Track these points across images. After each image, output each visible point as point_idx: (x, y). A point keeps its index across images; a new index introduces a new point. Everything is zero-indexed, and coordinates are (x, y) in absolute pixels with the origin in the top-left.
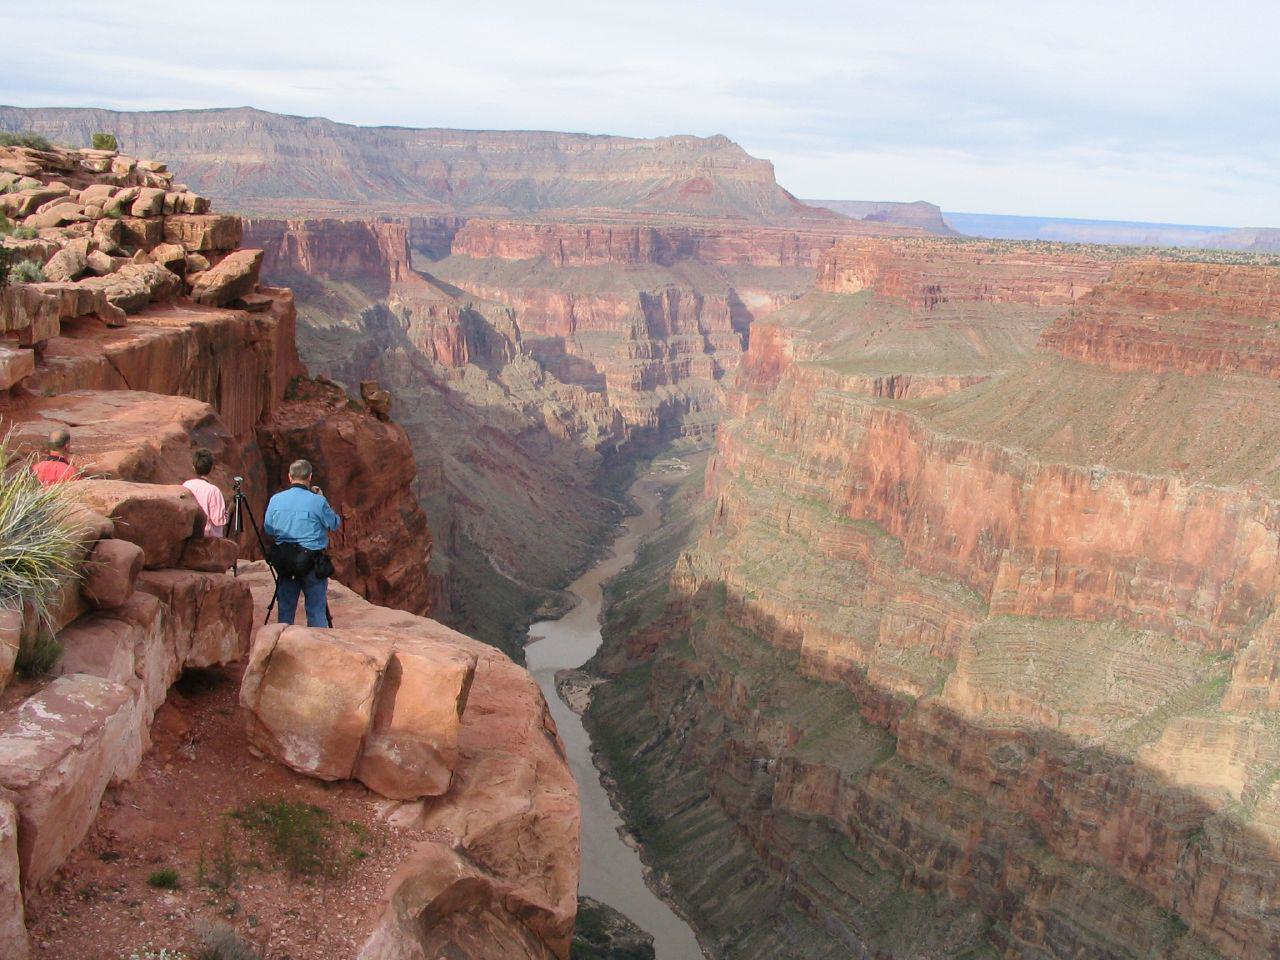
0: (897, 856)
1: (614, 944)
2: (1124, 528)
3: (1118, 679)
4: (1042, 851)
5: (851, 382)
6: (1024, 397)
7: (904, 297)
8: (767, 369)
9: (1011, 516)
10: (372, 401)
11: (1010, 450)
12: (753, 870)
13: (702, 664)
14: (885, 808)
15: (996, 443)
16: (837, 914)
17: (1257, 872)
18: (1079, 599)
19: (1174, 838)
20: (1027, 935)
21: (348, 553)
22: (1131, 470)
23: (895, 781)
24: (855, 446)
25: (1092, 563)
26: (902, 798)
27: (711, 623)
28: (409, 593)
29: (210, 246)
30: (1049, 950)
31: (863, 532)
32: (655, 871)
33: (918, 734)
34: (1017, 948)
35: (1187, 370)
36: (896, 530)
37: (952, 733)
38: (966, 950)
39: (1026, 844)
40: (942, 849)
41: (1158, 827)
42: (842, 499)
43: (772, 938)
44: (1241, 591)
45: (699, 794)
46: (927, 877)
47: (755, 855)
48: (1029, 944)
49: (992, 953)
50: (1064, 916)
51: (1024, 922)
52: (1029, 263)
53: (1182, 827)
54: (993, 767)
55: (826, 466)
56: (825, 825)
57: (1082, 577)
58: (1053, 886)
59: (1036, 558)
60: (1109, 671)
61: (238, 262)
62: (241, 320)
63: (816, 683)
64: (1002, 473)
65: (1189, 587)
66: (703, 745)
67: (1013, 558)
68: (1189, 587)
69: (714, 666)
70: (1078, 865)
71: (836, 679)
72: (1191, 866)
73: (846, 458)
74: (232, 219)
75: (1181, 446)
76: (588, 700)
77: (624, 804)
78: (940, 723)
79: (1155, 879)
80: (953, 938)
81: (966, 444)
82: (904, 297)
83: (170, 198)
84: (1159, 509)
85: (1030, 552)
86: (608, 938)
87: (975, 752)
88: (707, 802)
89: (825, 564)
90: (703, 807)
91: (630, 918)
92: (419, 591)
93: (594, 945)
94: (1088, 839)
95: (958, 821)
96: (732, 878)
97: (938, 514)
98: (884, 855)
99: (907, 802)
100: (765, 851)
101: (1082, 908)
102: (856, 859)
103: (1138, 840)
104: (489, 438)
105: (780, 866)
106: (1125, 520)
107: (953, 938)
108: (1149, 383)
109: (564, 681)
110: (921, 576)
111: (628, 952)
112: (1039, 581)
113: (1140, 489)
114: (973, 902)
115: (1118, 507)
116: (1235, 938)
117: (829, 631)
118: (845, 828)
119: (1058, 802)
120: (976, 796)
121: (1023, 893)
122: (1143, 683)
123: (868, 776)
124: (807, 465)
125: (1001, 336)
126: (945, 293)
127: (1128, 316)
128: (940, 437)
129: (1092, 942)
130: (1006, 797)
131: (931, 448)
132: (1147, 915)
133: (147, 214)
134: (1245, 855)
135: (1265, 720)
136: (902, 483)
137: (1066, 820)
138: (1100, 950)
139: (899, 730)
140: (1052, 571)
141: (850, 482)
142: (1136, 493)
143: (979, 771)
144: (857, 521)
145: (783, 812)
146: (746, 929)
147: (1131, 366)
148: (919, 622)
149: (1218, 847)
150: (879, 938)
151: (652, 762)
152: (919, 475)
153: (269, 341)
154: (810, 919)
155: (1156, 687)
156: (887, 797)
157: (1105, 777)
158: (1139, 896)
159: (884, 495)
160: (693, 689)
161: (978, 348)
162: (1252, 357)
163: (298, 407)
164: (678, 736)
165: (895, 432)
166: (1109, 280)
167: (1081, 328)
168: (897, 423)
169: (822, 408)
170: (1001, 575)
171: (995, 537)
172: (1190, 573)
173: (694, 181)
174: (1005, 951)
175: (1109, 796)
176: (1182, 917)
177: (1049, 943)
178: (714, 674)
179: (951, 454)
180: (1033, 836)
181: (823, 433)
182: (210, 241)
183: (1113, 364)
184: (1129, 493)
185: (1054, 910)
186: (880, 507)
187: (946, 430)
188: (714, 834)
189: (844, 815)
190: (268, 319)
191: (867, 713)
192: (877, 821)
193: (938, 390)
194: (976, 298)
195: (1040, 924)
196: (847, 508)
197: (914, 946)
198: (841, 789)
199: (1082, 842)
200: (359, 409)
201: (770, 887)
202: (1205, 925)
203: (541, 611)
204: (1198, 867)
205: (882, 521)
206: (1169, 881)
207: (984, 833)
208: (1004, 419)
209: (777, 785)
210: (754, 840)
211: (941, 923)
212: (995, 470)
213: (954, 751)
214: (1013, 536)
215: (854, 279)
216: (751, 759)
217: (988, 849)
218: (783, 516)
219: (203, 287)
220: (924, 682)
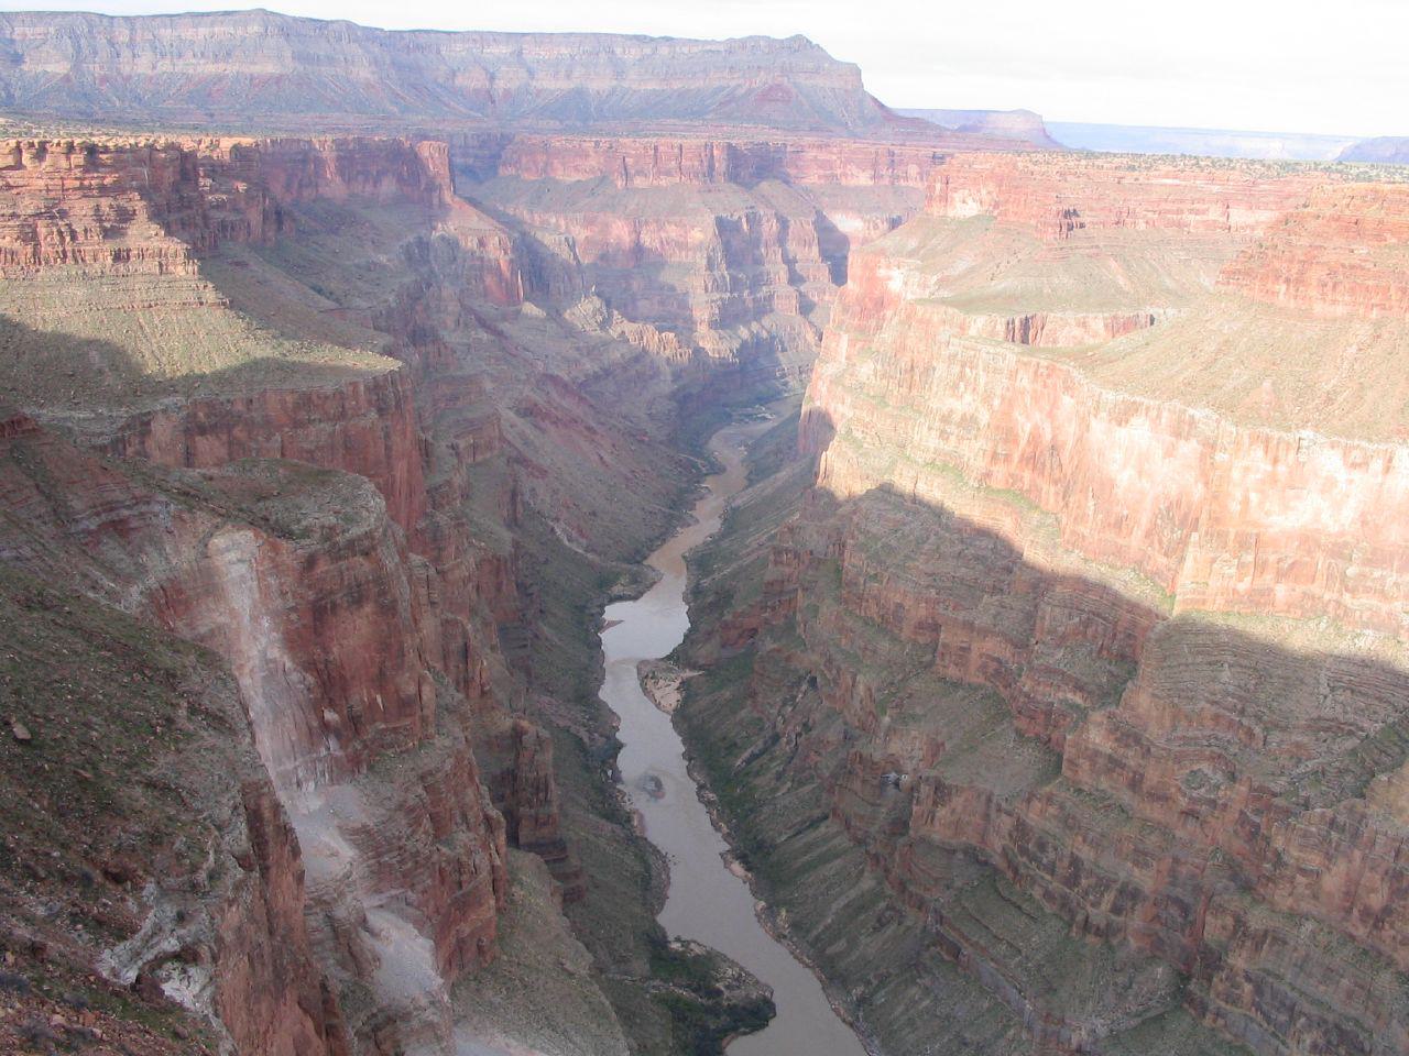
0: (1065, 897)
1: (728, 999)
3: (1333, 689)
5: (978, 323)
8: (870, 306)
9: (1198, 491)
11: (1198, 413)
12: (888, 908)
13: (815, 658)
14: (1051, 840)
15: (1177, 404)
16: (992, 964)
18: (1281, 591)
20: (1233, 1000)
22: (1347, 437)
23: (1062, 808)
25: (1299, 546)
26: (1071, 828)
27: (824, 609)
30: (1259, 1017)
31: (1006, 504)
32: (769, 907)
33: (1089, 752)
34: (1218, 1014)
36: (1047, 504)
37: (1131, 753)
38: (1152, 1013)
39: (1226, 889)
40: (1121, 892)
42: (980, 464)
43: (914, 992)
45: (817, 813)
48: (1235, 1009)
49: (1188, 1019)
50: (1279, 977)
51: (1228, 984)
52: (1177, 182)
54: (1184, 795)
55: (959, 425)
56: (975, 856)
58: (1263, 942)
59: (1231, 544)
60: (1323, 680)
63: (956, 685)
66: (820, 754)
67: (1203, 543)
69: (830, 661)
70: (1296, 917)
71: (981, 680)
73: (984, 417)
76: (679, 697)
77: (728, 823)
78: (1117, 740)
79: (1394, 938)
82: (1033, 222)
84: (1381, 485)
86: (719, 993)
88: (828, 822)
89: (962, 542)
90: (822, 829)
91: (742, 964)
93: (704, 1001)
94: (1307, 886)
95: (1141, 857)
96: (862, 917)
99: (1077, 834)
100: (902, 886)
101: (1301, 967)
102: (1014, 899)
103: (1374, 890)
104: (550, 388)
105: (921, 905)
106: (1339, 497)
107: (1136, 996)
108: (1362, 331)
109: (648, 674)
110: (1086, 560)
111: (744, 1008)
112: (1233, 570)
113: (1358, 461)
114: (1158, 953)
115: (1330, 483)
118: (997, 860)
119: (1267, 840)
120: (1165, 831)
121: (1226, 949)
123: (1029, 801)
125: (1147, 267)
128: (1110, 396)
130: (1198, 830)
131: (1097, 409)
132: (1385, 979)
136: (1054, 448)
138: (1325, 1022)
139: (1066, 747)
140: (1250, 558)
141: (990, 444)
142: (1354, 466)
143: (1165, 798)
144: (999, 491)
145: (923, 840)
146: (883, 980)
147: (1340, 310)
148: (1084, 616)
150: (1048, 997)
151: (757, 774)
152: (1080, 439)
154: (960, 969)
155: (1380, 699)
156: (1052, 826)
157: (1329, 812)
159: (1032, 460)
160: (804, 687)
161: (1121, 281)
164: (788, 743)
165: (1045, 386)
166: (1305, 206)
167: (1277, 264)
168: (1049, 376)
170: (1189, 563)
173: (771, 88)
174: (1204, 1016)
175: (1334, 835)
177: (1259, 1008)
178: (830, 671)
179: (1122, 416)
180: (1234, 877)
181: (956, 386)
183: (1318, 308)
184: (1345, 463)
185: (1265, 970)
186: (1027, 475)
187: (1116, 386)
188: (838, 863)
189: (997, 843)
191: (1022, 724)
192: (1039, 854)
193: (1078, 332)
194: (1117, 223)
195: (1248, 987)
196: (988, 475)
197: (1090, 1007)
198: (993, 815)
199: (1300, 889)
201: (909, 928)
205: (1029, 491)
207: (1173, 873)
208: (1186, 374)
209: (915, 808)
210: (887, 871)
211: (1121, 979)
212: (1178, 435)
213: (1135, 773)
215: (970, 201)
216: (880, 775)
217: (1178, 892)
220: (1093, 687)
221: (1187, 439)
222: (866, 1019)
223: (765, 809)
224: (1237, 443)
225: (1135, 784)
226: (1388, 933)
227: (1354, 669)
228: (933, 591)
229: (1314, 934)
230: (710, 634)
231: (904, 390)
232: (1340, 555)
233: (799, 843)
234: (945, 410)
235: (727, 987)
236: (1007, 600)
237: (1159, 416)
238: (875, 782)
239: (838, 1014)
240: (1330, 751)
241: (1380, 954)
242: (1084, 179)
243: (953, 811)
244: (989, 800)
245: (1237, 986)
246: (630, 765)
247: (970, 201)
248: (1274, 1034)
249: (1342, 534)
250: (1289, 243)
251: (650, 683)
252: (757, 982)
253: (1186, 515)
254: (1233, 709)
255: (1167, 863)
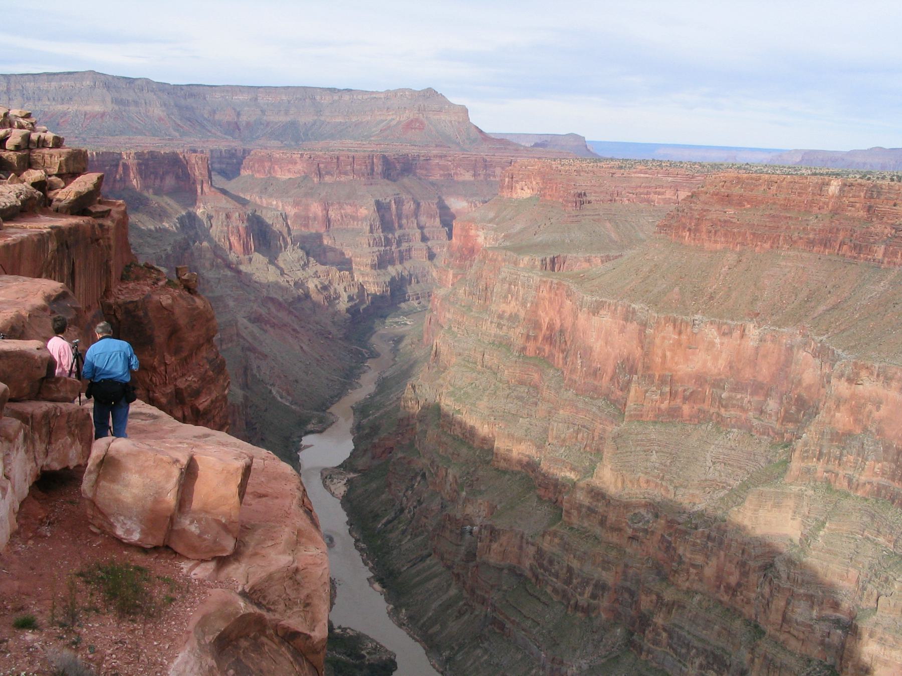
0: (564, 591)
2: (716, 359)
3: (714, 463)
4: (665, 584)
5: (525, 260)
6: (646, 269)
7: (561, 200)
8: (466, 253)
9: (638, 352)
10: (186, 280)
11: (636, 306)
12: (465, 604)
13: (425, 461)
15: (626, 302)
17: (811, 592)
19: (755, 571)
20: (656, 643)
21: (169, 389)
23: (562, 538)
24: (529, 305)
26: (567, 550)
27: (430, 432)
28: (214, 417)
29: (64, 171)
32: (396, 608)
35: (757, 249)
38: (613, 655)
39: (654, 580)
40: (596, 586)
41: (742, 564)
42: (520, 342)
43: (479, 652)
44: (797, 400)
45: (425, 552)
46: (586, 605)
47: (465, 594)
49: (633, 656)
50: (681, 628)
53: (760, 563)
54: (630, 527)
56: (513, 571)
57: (688, 393)
59: (656, 381)
61: (84, 183)
62: (88, 223)
63: (505, 472)
64: (631, 322)
65: (762, 398)
66: (427, 518)
68: (762, 398)
69: (433, 462)
70: (690, 592)
71: (519, 468)
72: (767, 590)
73: (522, 314)
74: (80, 151)
75: (755, 300)
76: (345, 489)
77: (372, 561)
78: (592, 497)
80: (605, 646)
81: (606, 302)
82: (561, 200)
83: (34, 137)
84: (740, 345)
85: (651, 377)
86: (364, 657)
87: (617, 517)
90: (428, 561)
92: (221, 414)
94: (697, 574)
95: (606, 565)
97: (587, 352)
98: (555, 590)
100: (472, 591)
103: (731, 574)
104: (270, 305)
105: (483, 601)
107: (605, 646)
108: (731, 258)
109: (327, 476)
110: (577, 395)
112: (658, 397)
113: (726, 331)
114: (619, 621)
115: (712, 344)
116: (797, 638)
117: (513, 436)
118: (528, 573)
119: (675, 549)
121: (652, 613)
122: (731, 465)
123: (543, 536)
124: (495, 320)
126: (589, 198)
127: (716, 212)
128: (588, 298)
129: (700, 645)
131: (581, 306)
132: (738, 623)
133: (17, 148)
134: (803, 581)
135: (814, 489)
136: (562, 332)
137: (681, 562)
138: (705, 650)
140: (667, 389)
141: (525, 330)
142: (724, 334)
143: (620, 530)
145: (484, 563)
147: (719, 246)
148: (576, 428)
149: (784, 576)
151: (391, 532)
152: (574, 324)
153: (109, 238)
154: (505, 637)
155: (740, 468)
157: (707, 531)
158: (732, 612)
159: (549, 339)
160: (419, 478)
161: (613, 235)
162: (801, 238)
163: (131, 285)
164: (409, 512)
165: (556, 295)
167: (683, 220)
168: (558, 288)
169: (505, 279)
171: (628, 367)
172: (762, 388)
175: (710, 544)
176: (761, 625)
177: (671, 647)
179: (596, 309)
180: (659, 573)
181: (506, 297)
182: (64, 167)
183: (707, 245)
186: (547, 348)
188: (436, 580)
189: (527, 563)
190: (108, 223)
191: (541, 492)
193: (585, 265)
195: (664, 635)
196: (524, 349)
197: (578, 653)
198: (524, 545)
199: (692, 577)
200: (175, 286)
201: (477, 616)
202: (776, 630)
204: (771, 591)
205: (548, 357)
206: (752, 601)
207: (625, 573)
209: (479, 544)
210: (464, 583)
211: (596, 637)
212: (626, 319)
213: (602, 516)
214: (640, 365)
215: (525, 188)
216: (460, 527)
217: (628, 584)
218: (480, 357)
219: (59, 200)
220: (580, 469)
221: (631, 322)
222: (450, 669)
223: (395, 552)
224: (658, 323)
225: (602, 523)
226: (739, 598)
227: (725, 451)
228: (492, 418)
229: (700, 602)
230: (365, 451)
231: (482, 302)
232: (718, 386)
233: (414, 571)
234: (500, 311)
235: (368, 653)
236: (534, 421)
237: (616, 309)
238: (458, 532)
239: (434, 667)
240: (712, 498)
241: (735, 610)
242: (591, 174)
243: (501, 545)
244: (522, 537)
245: (658, 634)
247: (525, 188)
248: (680, 661)
249: (719, 374)
250: (691, 209)
251: (328, 482)
252: (387, 651)
253: (632, 366)
254: (658, 477)
255: (620, 569)
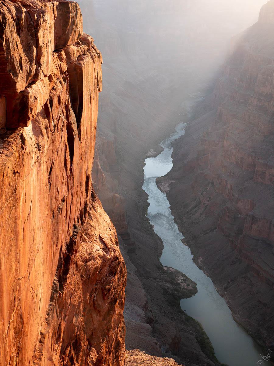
86: (179, 284)
109: (159, 181)
160: (210, 185)
203: (149, 154)
246: (152, 210)
